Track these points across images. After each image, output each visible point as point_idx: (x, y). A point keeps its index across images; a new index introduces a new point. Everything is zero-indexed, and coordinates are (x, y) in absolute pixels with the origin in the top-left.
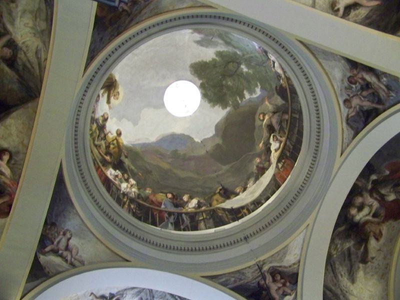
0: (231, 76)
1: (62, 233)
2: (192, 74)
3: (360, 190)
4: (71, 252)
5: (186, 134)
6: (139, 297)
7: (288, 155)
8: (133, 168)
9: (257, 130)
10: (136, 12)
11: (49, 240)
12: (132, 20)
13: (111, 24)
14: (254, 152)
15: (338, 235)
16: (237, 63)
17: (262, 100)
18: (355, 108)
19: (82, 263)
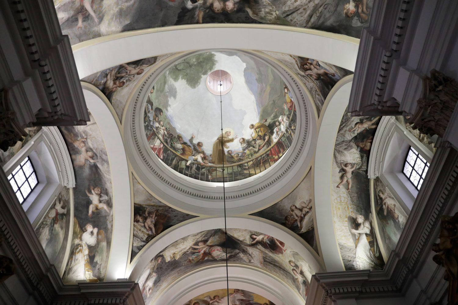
1: (292, 213)
3: (207, 11)
4: (304, 207)
5: (243, 74)
6: (343, 151)
8: (272, 116)
10: (154, 208)
11: (294, 223)
12: (160, 206)
13: (166, 216)
15: (257, 14)
16: (176, 67)
18: (139, 68)
19: (310, 201)
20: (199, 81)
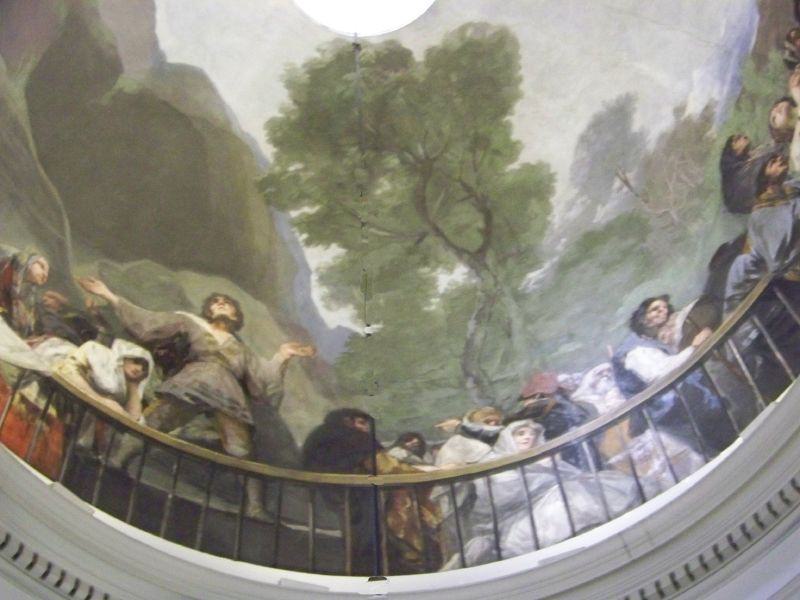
0: (420, 202)
2: (463, 29)
7: (81, 441)
9: (165, 276)
14: (71, 254)
16: (482, 251)
17: (300, 328)
20: (457, 44)
